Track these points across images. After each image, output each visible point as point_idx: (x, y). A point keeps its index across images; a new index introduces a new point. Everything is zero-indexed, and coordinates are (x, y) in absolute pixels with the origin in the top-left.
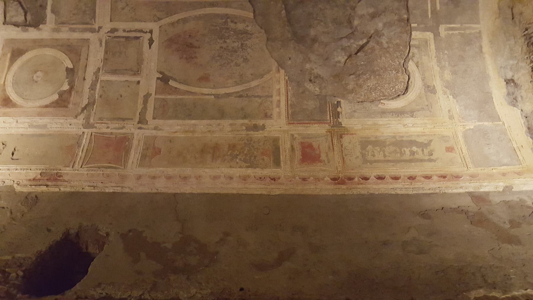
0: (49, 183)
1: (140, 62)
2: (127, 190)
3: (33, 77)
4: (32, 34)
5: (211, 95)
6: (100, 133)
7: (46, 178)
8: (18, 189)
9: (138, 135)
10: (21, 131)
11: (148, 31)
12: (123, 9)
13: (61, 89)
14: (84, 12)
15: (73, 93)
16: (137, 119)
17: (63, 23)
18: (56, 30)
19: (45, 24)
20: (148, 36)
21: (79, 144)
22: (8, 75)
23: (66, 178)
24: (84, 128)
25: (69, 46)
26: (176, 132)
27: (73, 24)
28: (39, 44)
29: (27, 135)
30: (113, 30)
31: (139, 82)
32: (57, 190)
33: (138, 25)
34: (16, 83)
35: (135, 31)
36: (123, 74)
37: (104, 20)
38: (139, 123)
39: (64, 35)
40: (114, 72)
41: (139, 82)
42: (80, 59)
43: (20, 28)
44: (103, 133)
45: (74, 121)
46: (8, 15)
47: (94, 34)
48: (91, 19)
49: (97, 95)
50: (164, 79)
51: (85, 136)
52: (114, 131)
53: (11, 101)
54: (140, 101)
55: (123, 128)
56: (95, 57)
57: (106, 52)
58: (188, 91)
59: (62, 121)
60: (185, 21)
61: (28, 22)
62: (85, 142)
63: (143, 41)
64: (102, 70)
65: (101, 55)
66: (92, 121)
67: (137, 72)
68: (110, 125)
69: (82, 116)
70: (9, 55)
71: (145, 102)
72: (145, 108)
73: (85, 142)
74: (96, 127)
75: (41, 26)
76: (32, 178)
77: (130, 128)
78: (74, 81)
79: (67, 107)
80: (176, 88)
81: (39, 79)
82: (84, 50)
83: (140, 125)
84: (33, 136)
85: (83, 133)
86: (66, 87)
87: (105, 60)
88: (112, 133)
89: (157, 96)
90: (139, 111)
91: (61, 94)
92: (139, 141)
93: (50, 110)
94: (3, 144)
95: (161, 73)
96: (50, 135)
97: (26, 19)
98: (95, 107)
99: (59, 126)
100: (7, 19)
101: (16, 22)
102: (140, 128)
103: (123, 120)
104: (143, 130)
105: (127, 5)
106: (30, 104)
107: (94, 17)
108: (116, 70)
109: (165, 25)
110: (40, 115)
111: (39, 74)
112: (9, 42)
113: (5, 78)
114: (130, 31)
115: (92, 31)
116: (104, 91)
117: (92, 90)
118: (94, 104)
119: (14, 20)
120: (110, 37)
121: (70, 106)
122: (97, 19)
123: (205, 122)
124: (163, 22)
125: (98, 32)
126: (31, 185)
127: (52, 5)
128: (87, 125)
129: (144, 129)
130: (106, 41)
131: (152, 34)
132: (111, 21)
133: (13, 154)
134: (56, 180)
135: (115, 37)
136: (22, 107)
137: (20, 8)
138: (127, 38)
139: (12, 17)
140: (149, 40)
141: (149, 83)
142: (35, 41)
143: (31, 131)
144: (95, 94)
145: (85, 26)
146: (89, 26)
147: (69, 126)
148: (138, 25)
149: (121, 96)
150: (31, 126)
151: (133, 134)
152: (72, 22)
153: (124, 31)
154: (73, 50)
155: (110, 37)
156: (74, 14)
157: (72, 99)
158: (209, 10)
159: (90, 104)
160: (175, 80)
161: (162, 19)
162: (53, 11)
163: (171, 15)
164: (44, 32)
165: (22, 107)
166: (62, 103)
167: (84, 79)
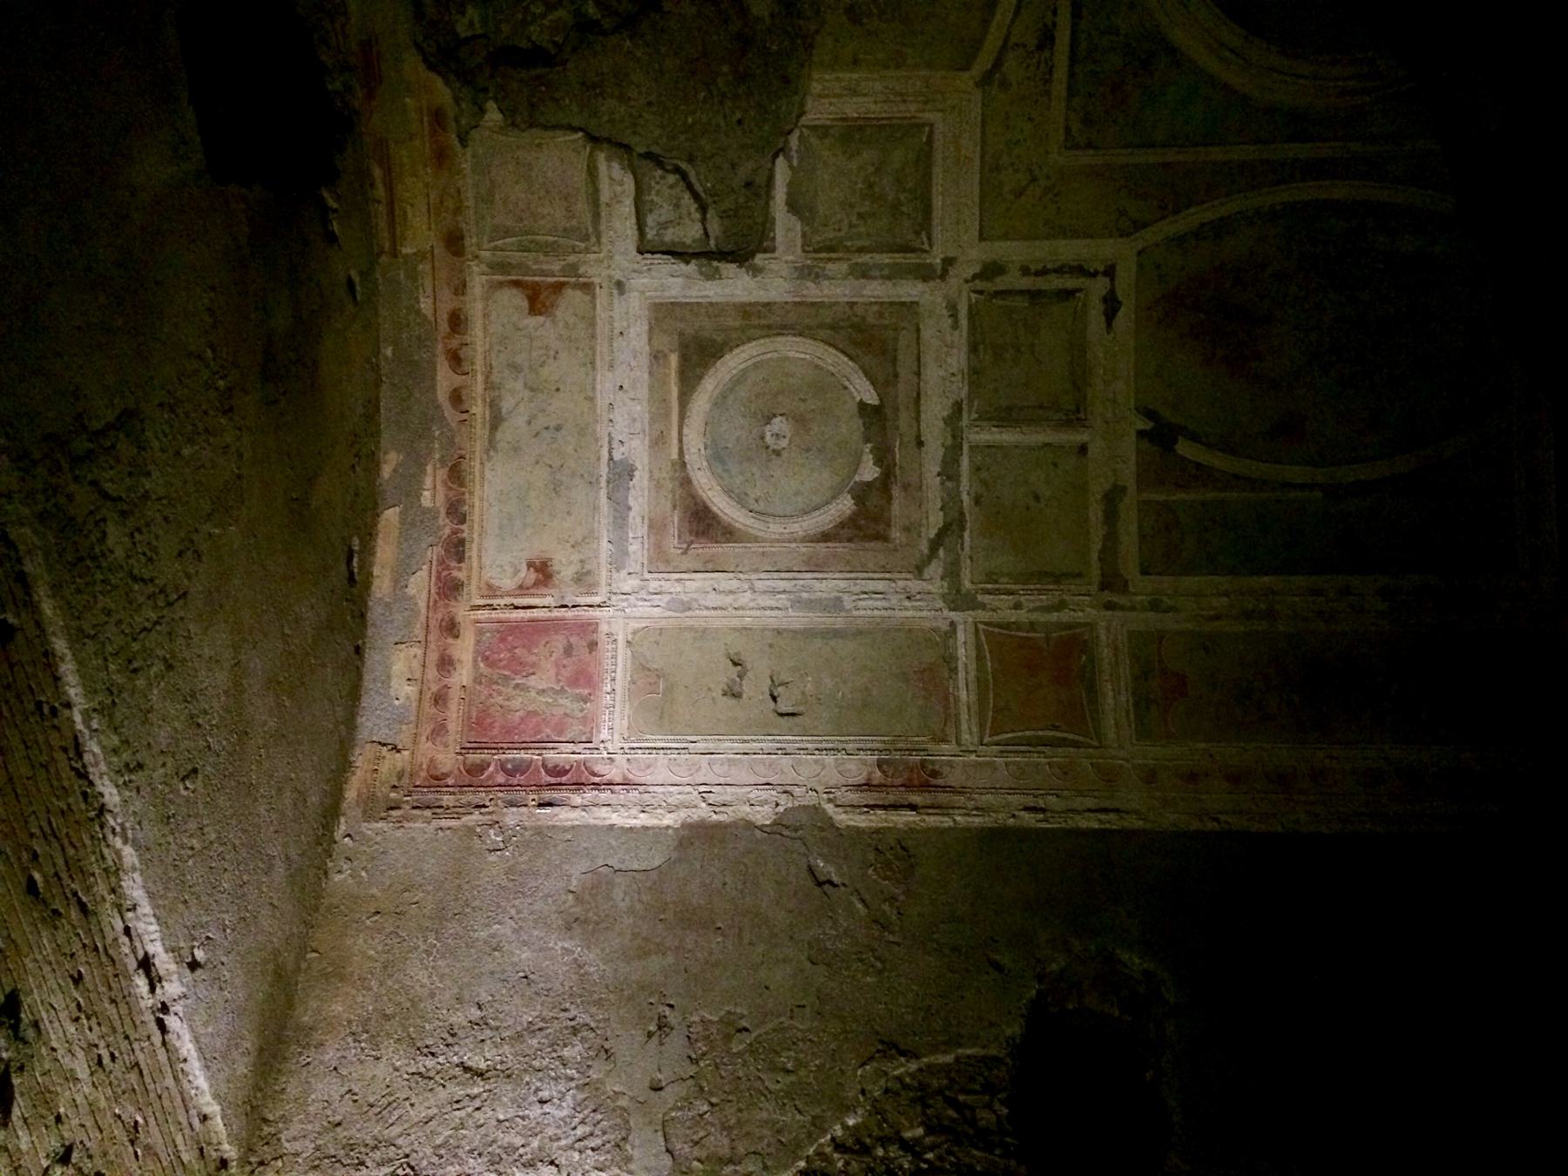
0: (916, 798)
1: (1079, 378)
2: (1134, 823)
3: (762, 438)
4: (735, 286)
5: (1312, 487)
6: (999, 626)
7: (899, 781)
8: (842, 818)
9: (1111, 631)
10: (773, 619)
11: (1101, 268)
12: (1019, 193)
13: (857, 478)
14: (895, 206)
15: (896, 492)
16: (1095, 573)
17: (831, 249)
18: (806, 273)
19: (773, 250)
20: (1100, 286)
21: (950, 661)
22: (685, 430)
23: (954, 778)
24: (951, 610)
25: (857, 327)
26: (1217, 618)
27: (861, 250)
28: (758, 320)
29: (795, 632)
30: (992, 270)
31: (1083, 449)
32: (946, 822)
33: (1068, 250)
34: (717, 455)
35: (1059, 271)
36: (1031, 422)
37: (957, 235)
38: (1103, 587)
39: (837, 289)
40: (1005, 417)
41: (1083, 449)
42: (896, 375)
43: (692, 267)
44: (1007, 626)
45: (915, 585)
46: (650, 220)
47: (932, 284)
48: (917, 233)
49: (965, 497)
50: (1161, 435)
51: (961, 636)
52: (1035, 616)
53: (715, 517)
54: (1095, 513)
55: (1060, 606)
56: (943, 367)
57: (973, 349)
58: (1236, 477)
59: (880, 586)
60: (1220, 228)
61: (712, 242)
62: (964, 653)
63: (1085, 305)
64: (970, 412)
65: (958, 360)
66: (967, 584)
67: (1075, 417)
68: (1022, 599)
69: (935, 569)
70: (674, 359)
71: (1111, 516)
72: (1111, 538)
73: (964, 653)
74: (983, 606)
75: (759, 259)
76: (861, 780)
77: (1082, 609)
78: (889, 450)
79: (882, 537)
80: (1198, 466)
81: (784, 443)
82: (905, 339)
83: (1107, 596)
84: (808, 634)
85: (952, 624)
86: (869, 472)
87: (975, 374)
88: (1032, 626)
89: (1145, 496)
90: (1096, 546)
91: (862, 493)
92: (1116, 649)
93: (840, 548)
94: (735, 664)
95: (1150, 414)
96: (860, 633)
97: (706, 234)
98: (966, 534)
99: (879, 604)
100: (651, 234)
101: (673, 243)
102: (1110, 606)
103: (1057, 578)
104: (1119, 614)
105: (1034, 179)
106: (775, 528)
107: (924, 222)
108: (1010, 409)
109: (1157, 245)
110: (816, 566)
111: (778, 424)
112: (663, 313)
113: (680, 441)
114: (1043, 272)
115: (924, 274)
116: (984, 483)
117: (949, 478)
118: (963, 529)
119: (670, 236)
120: (981, 292)
121: (896, 534)
122: (937, 233)
123: (1300, 581)
124: (1149, 236)
125: (943, 277)
126: (872, 807)
127: (790, 185)
128: (958, 600)
129: (1123, 608)
130: (970, 306)
131: (1112, 279)
132: (982, 238)
133: (774, 699)
134: (925, 787)
135: (997, 294)
136: (756, 539)
137: (687, 196)
138: (1034, 295)
139: (664, 226)
140: (1105, 300)
141: (1114, 451)
142: (746, 311)
143: (798, 619)
144: (959, 493)
145: (899, 258)
146: (912, 259)
147: (907, 603)
148: (1068, 250)
149: (1037, 498)
150: (798, 603)
151: (1091, 626)
152: (859, 243)
153: (1025, 271)
154: (870, 339)
155: (981, 292)
156: (860, 216)
157: (896, 508)
158: (1304, 192)
159: (952, 528)
160: (1194, 438)
161: (1145, 225)
162: (793, 206)
163: (1176, 212)
164: (770, 283)
165: (756, 539)
166: (866, 524)
167: (920, 444)
